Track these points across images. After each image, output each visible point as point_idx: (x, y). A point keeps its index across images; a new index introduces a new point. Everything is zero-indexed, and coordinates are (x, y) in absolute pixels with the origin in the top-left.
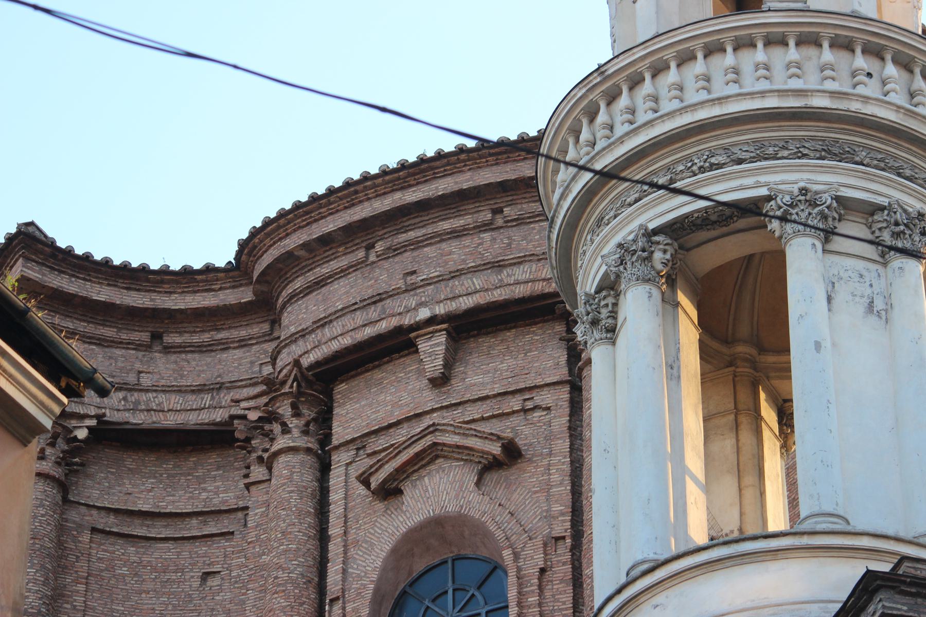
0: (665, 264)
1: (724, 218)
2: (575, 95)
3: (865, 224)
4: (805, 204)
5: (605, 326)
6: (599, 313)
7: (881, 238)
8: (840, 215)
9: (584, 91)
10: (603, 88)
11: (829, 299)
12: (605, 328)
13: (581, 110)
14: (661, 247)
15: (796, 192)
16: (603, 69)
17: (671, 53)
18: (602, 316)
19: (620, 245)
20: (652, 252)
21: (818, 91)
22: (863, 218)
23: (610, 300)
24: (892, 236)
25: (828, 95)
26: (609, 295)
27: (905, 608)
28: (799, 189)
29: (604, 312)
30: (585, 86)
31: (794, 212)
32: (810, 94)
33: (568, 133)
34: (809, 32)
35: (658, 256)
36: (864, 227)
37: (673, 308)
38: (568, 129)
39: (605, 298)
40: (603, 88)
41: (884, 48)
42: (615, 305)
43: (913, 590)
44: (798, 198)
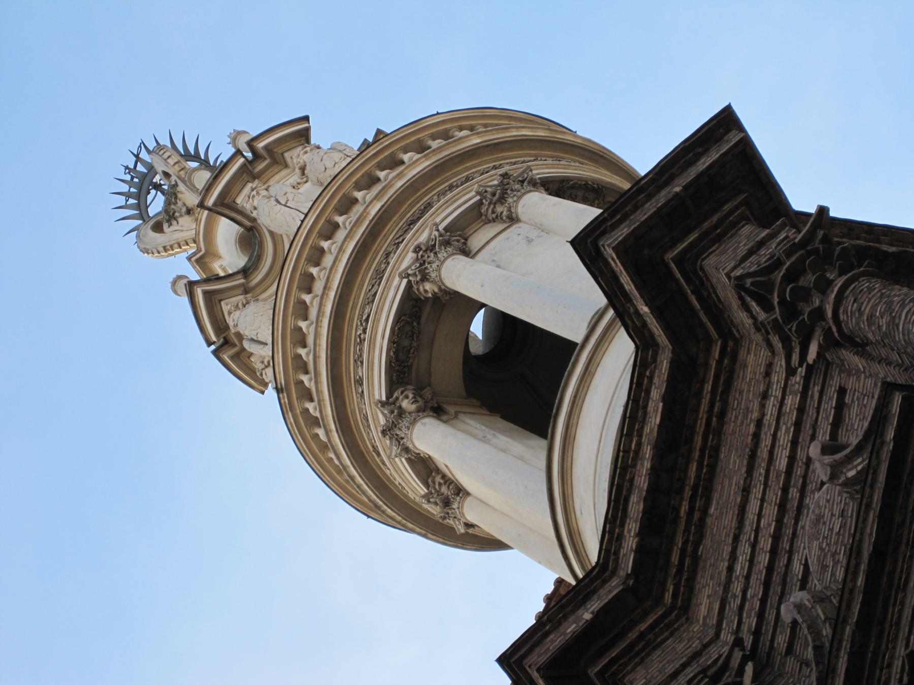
0: (415, 402)
1: (410, 333)
2: (291, 424)
3: (485, 224)
4: (427, 253)
5: (452, 494)
6: (443, 494)
7: (499, 215)
8: (460, 235)
9: (290, 414)
10: (294, 396)
11: (498, 266)
12: (454, 495)
13: (306, 428)
14: (401, 397)
15: (414, 255)
16: (279, 386)
17: (291, 320)
18: (446, 493)
19: (384, 433)
20: (400, 407)
21: (368, 206)
22: (479, 223)
23: (438, 479)
24: (502, 204)
25: (375, 201)
26: (434, 478)
27: (626, 229)
28: (414, 252)
29: (444, 489)
30: (287, 413)
31: (426, 265)
32: (365, 214)
33: (324, 452)
34: (339, 200)
35: (405, 404)
36: (486, 226)
37: (457, 419)
38: (320, 451)
39: (434, 483)
40: (294, 396)
41: (393, 155)
42: (444, 476)
43: (618, 217)
44: (419, 257)
